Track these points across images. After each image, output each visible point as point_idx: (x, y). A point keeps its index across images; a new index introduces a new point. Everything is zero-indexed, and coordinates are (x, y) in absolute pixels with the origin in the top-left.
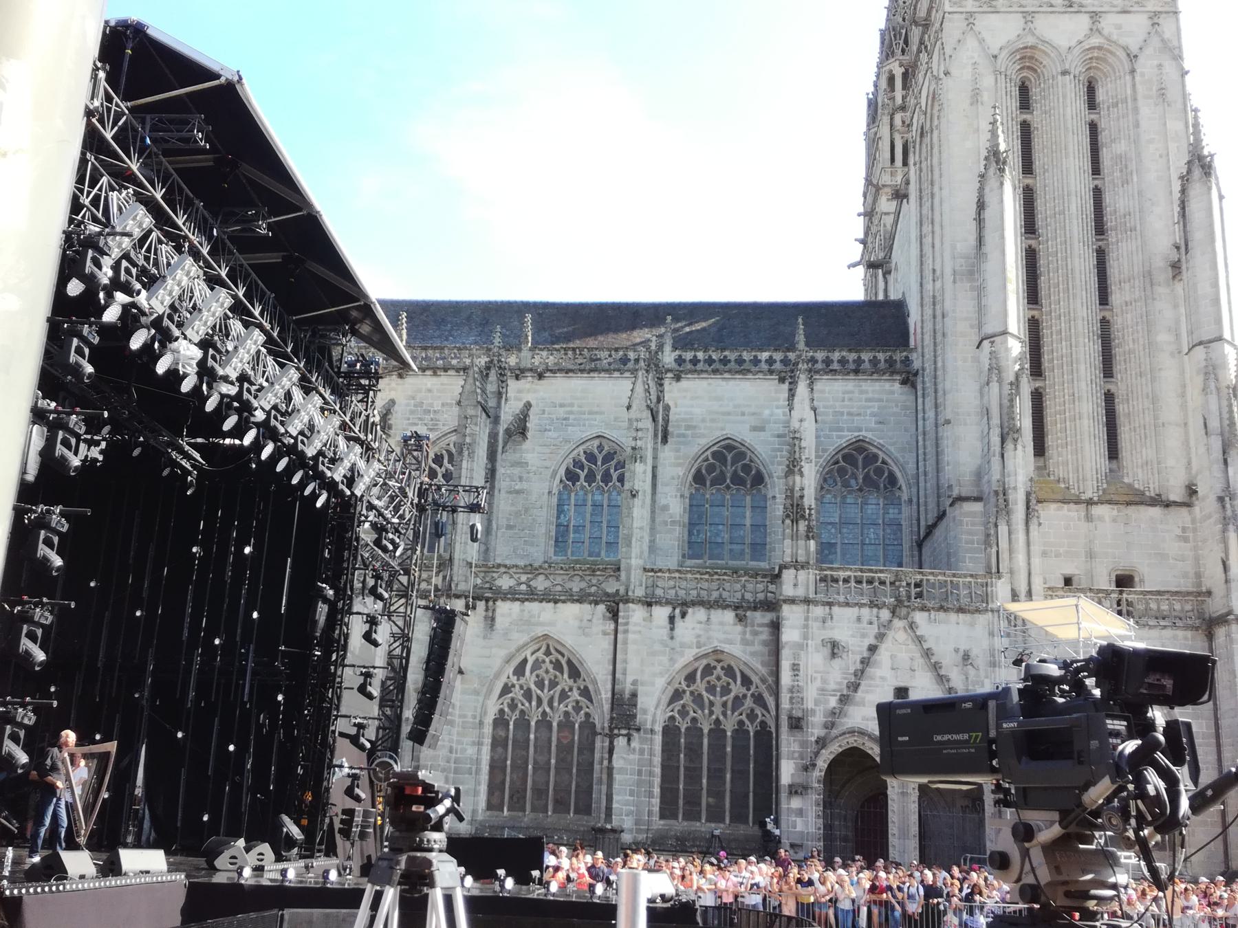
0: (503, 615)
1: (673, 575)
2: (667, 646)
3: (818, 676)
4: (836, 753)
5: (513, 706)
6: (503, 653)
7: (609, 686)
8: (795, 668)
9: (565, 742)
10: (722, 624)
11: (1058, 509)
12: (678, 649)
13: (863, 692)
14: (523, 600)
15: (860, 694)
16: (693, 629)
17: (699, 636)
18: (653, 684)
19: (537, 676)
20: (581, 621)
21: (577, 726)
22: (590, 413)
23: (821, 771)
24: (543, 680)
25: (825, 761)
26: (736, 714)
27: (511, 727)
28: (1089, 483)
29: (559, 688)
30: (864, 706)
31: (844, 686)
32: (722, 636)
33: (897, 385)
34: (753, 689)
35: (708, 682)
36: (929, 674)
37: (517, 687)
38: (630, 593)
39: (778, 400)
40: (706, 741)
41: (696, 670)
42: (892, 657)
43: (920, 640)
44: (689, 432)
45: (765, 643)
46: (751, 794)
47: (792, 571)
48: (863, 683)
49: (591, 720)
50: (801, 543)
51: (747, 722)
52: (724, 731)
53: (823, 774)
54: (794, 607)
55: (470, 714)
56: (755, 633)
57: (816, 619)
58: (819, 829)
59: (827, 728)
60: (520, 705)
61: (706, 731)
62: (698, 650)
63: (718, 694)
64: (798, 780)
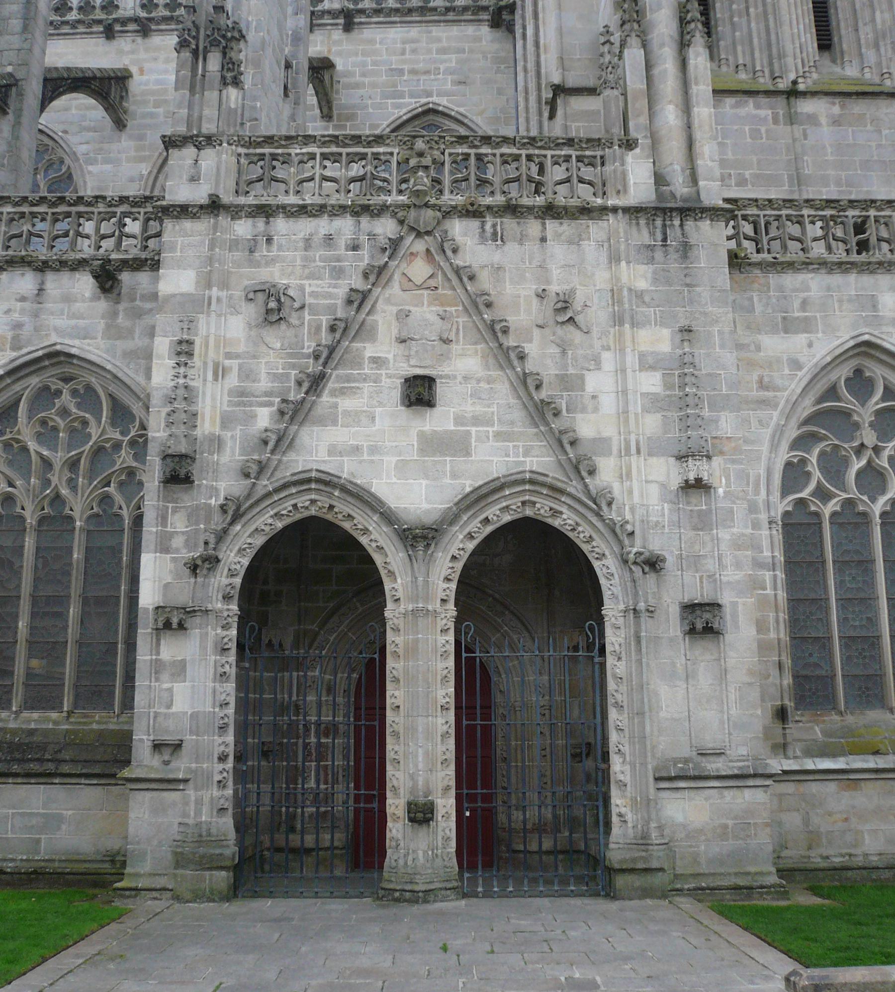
4: (269, 532)
11: (736, 106)
13: (333, 394)
15: (326, 398)
16: (8, 312)
17: (18, 326)
23: (232, 574)
25: (241, 551)
28: (790, 60)
30: (335, 423)
32: (61, 322)
33: (485, 30)
40: (29, 543)
42: (403, 316)
44: (160, 110)
47: (190, 152)
50: (212, 96)
51: (118, 498)
52: (70, 519)
53: (238, 581)
54: (188, 224)
59: (247, 475)
61: (31, 519)
62: (15, 354)
64: (183, 598)
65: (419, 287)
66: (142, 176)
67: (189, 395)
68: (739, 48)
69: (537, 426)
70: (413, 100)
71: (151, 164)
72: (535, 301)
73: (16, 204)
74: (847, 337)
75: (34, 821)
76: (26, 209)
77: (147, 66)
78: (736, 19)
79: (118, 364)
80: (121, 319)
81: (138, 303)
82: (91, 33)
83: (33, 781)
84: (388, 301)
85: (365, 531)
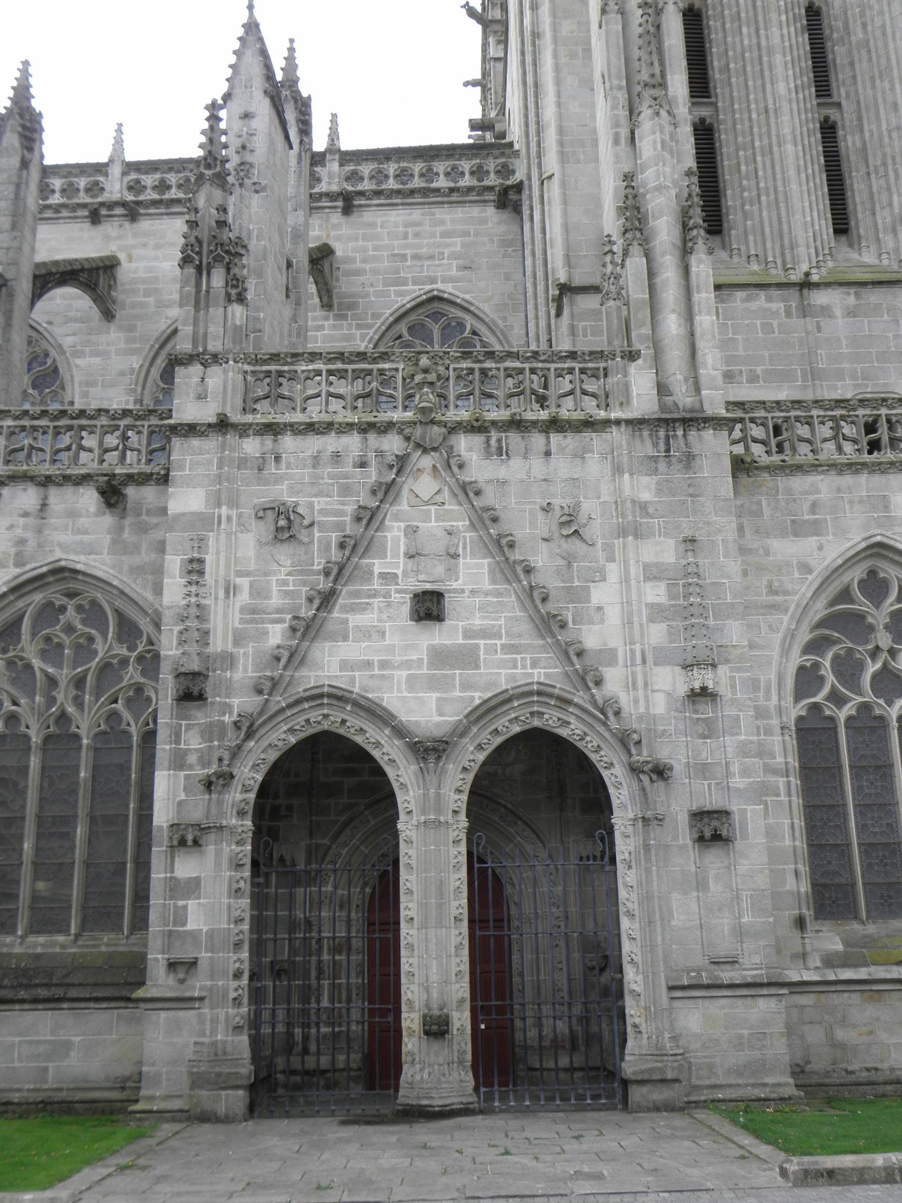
3: (244, 583)
4: (283, 747)
11: (748, 299)
16: (11, 527)
17: (22, 542)
23: (246, 790)
25: (255, 766)
28: (802, 250)
30: (345, 638)
35: (48, 639)
40: (34, 762)
42: (412, 531)
44: (151, 300)
47: (196, 369)
50: (216, 312)
51: (126, 715)
52: (77, 737)
53: (252, 796)
54: (195, 442)
58: (239, 921)
59: (260, 692)
61: (36, 739)
62: (18, 571)
64: (196, 814)
65: (427, 503)
66: (132, 370)
67: (202, 613)
68: (751, 238)
69: (544, 638)
70: (417, 287)
71: (142, 357)
72: (540, 515)
73: (17, 418)
74: (859, 539)
75: (41, 1049)
76: (26, 422)
77: (136, 252)
78: (747, 207)
79: (125, 579)
80: (126, 535)
81: (144, 517)
82: (76, 218)
83: (40, 1007)
84: (397, 518)
85: (378, 745)
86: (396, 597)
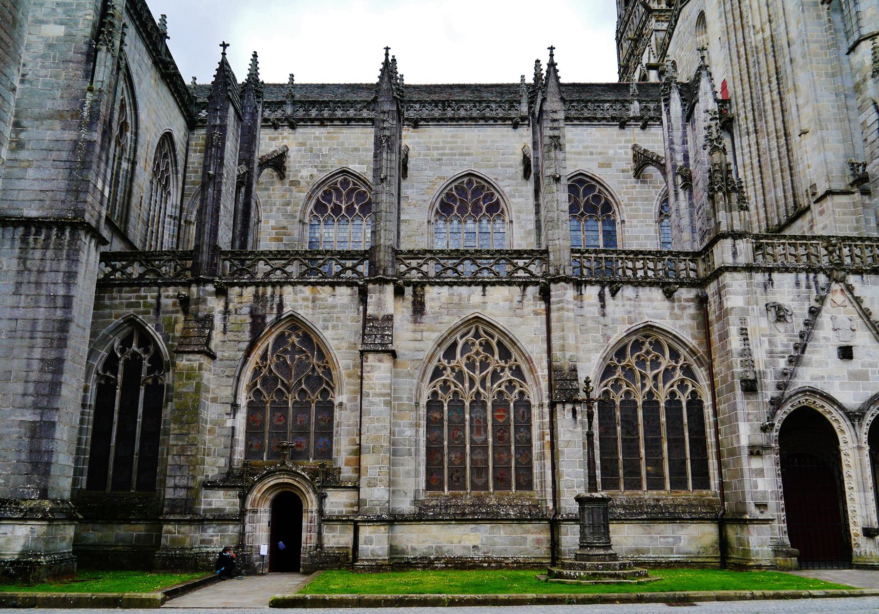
0: (432, 299)
1: (599, 256)
2: (599, 323)
3: (766, 339)
5: (445, 387)
6: (435, 336)
7: (545, 364)
8: (743, 332)
9: (501, 420)
10: (650, 300)
12: (611, 326)
13: (809, 353)
14: (451, 284)
16: (624, 305)
17: (629, 312)
18: (589, 360)
19: (468, 358)
20: (511, 301)
21: (512, 405)
22: (461, 154)
24: (474, 361)
26: (668, 385)
27: (446, 408)
29: (490, 369)
31: (792, 348)
32: (650, 311)
34: (681, 362)
36: (868, 333)
37: (449, 369)
38: (561, 272)
39: (620, 142)
41: (626, 346)
42: (833, 318)
43: (858, 300)
45: (693, 317)
46: (689, 462)
48: (809, 344)
49: (526, 398)
50: (735, 214)
51: (679, 393)
52: (657, 403)
54: (735, 275)
55: (405, 396)
56: (683, 308)
57: (758, 285)
60: (453, 387)
61: (640, 403)
62: (630, 326)
63: (648, 368)
65: (839, 306)
81: (683, 303)
86: (830, 348)
